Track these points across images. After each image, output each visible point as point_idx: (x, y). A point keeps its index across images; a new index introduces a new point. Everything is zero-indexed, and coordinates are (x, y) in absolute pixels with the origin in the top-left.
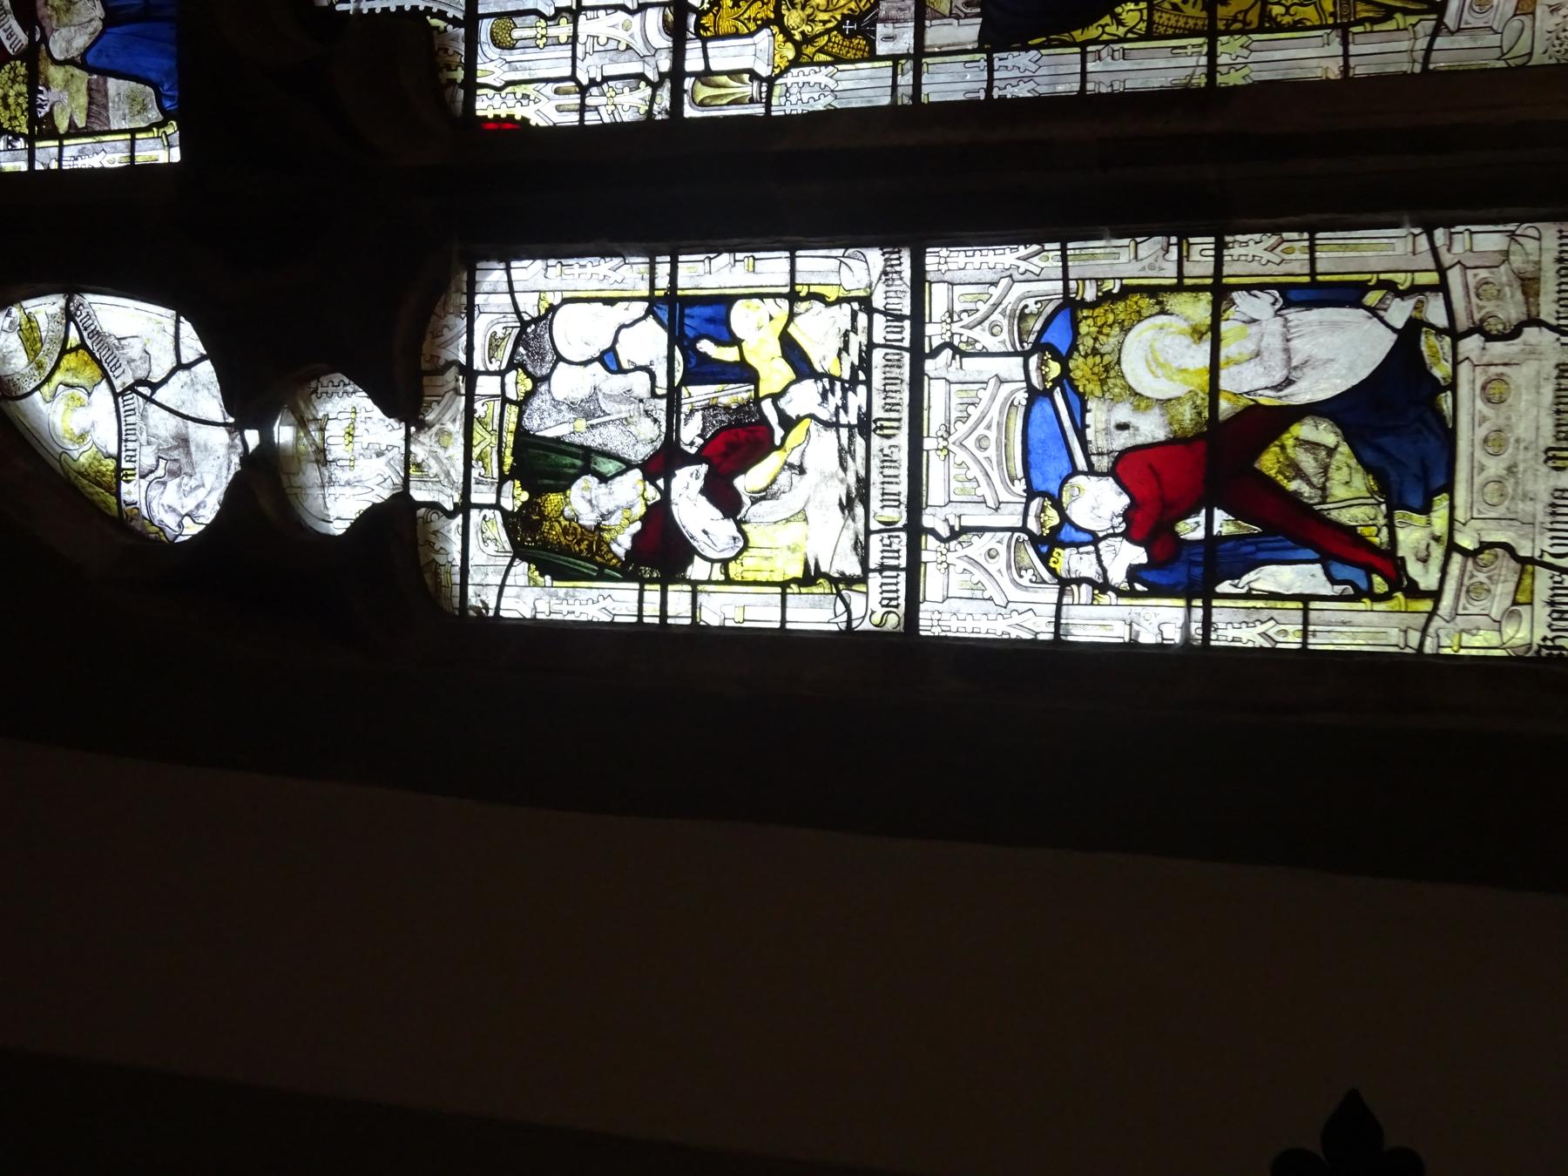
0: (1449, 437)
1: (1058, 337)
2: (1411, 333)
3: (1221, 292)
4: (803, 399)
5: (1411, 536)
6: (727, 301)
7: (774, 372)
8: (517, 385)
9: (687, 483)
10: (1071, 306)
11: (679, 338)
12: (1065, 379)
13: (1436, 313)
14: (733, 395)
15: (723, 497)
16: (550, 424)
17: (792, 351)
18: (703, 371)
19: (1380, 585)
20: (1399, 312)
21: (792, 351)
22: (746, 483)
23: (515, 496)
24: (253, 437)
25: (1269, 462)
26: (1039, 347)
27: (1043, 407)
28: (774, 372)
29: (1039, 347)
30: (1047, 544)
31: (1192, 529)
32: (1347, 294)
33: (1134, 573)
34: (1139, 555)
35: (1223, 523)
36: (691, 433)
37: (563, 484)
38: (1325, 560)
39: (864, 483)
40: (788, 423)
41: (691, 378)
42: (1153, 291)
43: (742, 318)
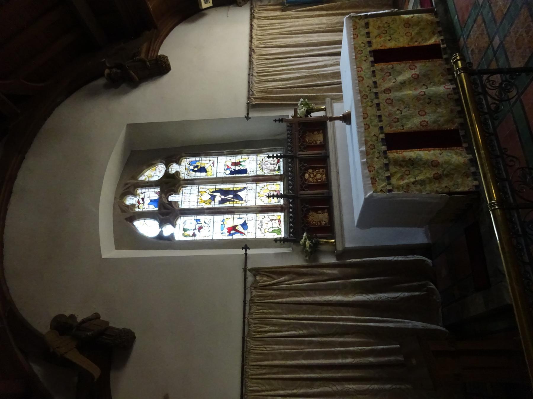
0: (247, 226)
1: (223, 221)
2: (245, 220)
3: (234, 218)
4: (205, 225)
5: (246, 232)
6: (200, 219)
7: (203, 223)
8: (184, 225)
9: (197, 230)
10: (224, 219)
11: (196, 221)
12: (223, 224)
13: (247, 219)
14: (200, 225)
15: (199, 231)
16: (185, 228)
17: (205, 222)
18: (198, 223)
19: (243, 235)
20: (245, 219)
21: (205, 222)
22: (200, 230)
23: (183, 232)
24: (161, 229)
25: (237, 228)
26: (222, 222)
27: (222, 225)
28: (203, 223)
29: (222, 222)
30: (222, 234)
31: (232, 232)
32: (242, 218)
33: (228, 235)
34: (228, 234)
35: (234, 232)
36: (197, 228)
37: (186, 231)
38: (240, 233)
39: (209, 230)
40: (204, 227)
41: (197, 224)
42: (229, 218)
43: (201, 220)
